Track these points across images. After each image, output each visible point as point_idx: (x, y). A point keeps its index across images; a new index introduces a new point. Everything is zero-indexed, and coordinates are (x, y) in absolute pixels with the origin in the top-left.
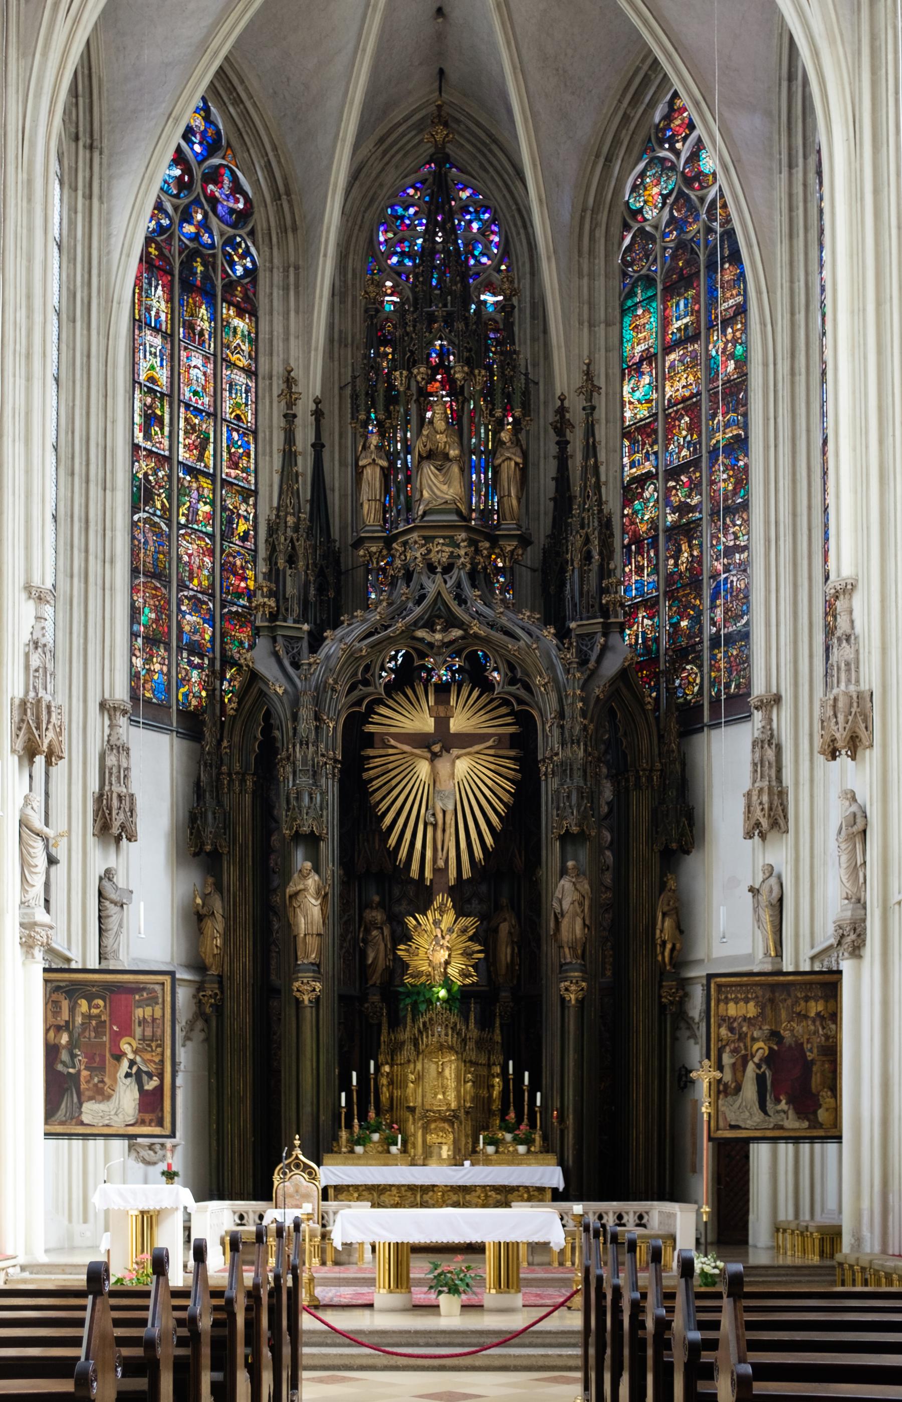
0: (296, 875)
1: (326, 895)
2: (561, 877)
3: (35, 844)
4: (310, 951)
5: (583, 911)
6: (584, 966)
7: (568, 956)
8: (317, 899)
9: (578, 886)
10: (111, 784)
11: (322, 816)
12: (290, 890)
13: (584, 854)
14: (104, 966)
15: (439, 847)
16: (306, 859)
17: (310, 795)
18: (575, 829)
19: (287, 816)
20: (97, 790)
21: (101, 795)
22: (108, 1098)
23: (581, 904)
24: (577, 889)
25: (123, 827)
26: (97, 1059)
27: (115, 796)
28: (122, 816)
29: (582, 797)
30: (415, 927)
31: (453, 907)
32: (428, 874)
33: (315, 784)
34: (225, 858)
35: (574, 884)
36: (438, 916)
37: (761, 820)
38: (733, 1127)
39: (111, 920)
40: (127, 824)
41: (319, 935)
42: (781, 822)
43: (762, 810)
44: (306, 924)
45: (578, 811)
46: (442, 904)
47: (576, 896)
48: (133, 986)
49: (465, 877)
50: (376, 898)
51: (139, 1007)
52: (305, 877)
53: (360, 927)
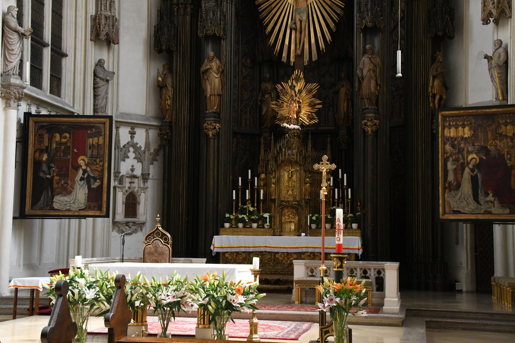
0: (206, 60)
1: (223, 72)
2: (363, 55)
3: (12, 37)
4: (213, 105)
5: (376, 76)
6: (378, 110)
7: (367, 104)
8: (217, 74)
9: (372, 60)
10: (101, 10)
11: (220, 25)
12: (203, 68)
13: (377, 42)
14: (96, 114)
15: (298, 42)
16: (213, 51)
17: (213, 11)
18: (369, 25)
19: (200, 25)
20: (94, 14)
21: (96, 17)
22: (70, 193)
23: (374, 71)
24: (371, 62)
25: (107, 35)
26: (64, 169)
27: (103, 17)
28: (107, 28)
29: (375, 5)
30: (281, 90)
31: (304, 77)
32: (292, 59)
33: (217, 5)
34: (175, 53)
35: (370, 59)
36: (294, 83)
37: (492, 10)
38: (458, 212)
39: (100, 89)
40: (110, 34)
41: (219, 95)
42: (507, 11)
43: (493, 3)
44: (211, 89)
45: (372, 14)
46: (297, 75)
47: (372, 66)
48: (87, 124)
49: (314, 60)
50: (268, 76)
51: (90, 138)
52: (211, 61)
53: (259, 93)
